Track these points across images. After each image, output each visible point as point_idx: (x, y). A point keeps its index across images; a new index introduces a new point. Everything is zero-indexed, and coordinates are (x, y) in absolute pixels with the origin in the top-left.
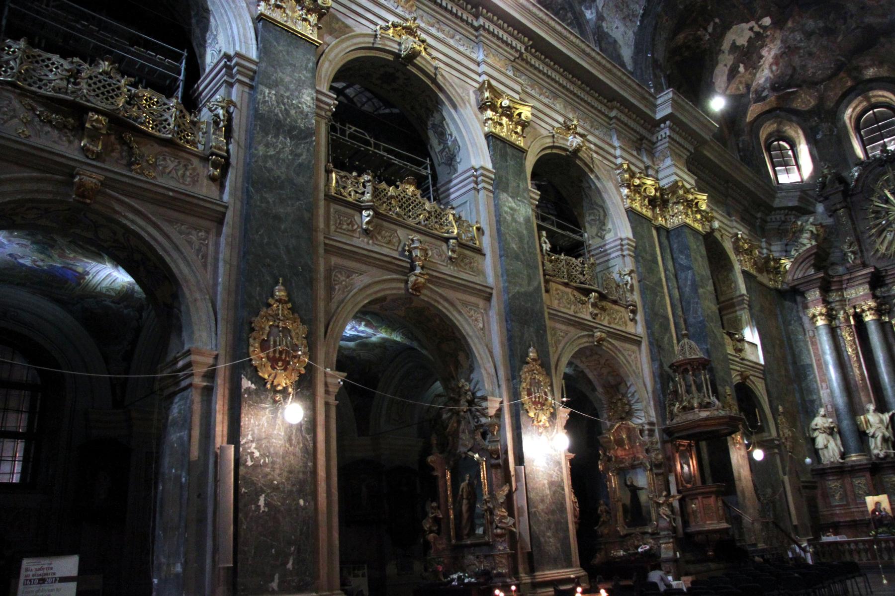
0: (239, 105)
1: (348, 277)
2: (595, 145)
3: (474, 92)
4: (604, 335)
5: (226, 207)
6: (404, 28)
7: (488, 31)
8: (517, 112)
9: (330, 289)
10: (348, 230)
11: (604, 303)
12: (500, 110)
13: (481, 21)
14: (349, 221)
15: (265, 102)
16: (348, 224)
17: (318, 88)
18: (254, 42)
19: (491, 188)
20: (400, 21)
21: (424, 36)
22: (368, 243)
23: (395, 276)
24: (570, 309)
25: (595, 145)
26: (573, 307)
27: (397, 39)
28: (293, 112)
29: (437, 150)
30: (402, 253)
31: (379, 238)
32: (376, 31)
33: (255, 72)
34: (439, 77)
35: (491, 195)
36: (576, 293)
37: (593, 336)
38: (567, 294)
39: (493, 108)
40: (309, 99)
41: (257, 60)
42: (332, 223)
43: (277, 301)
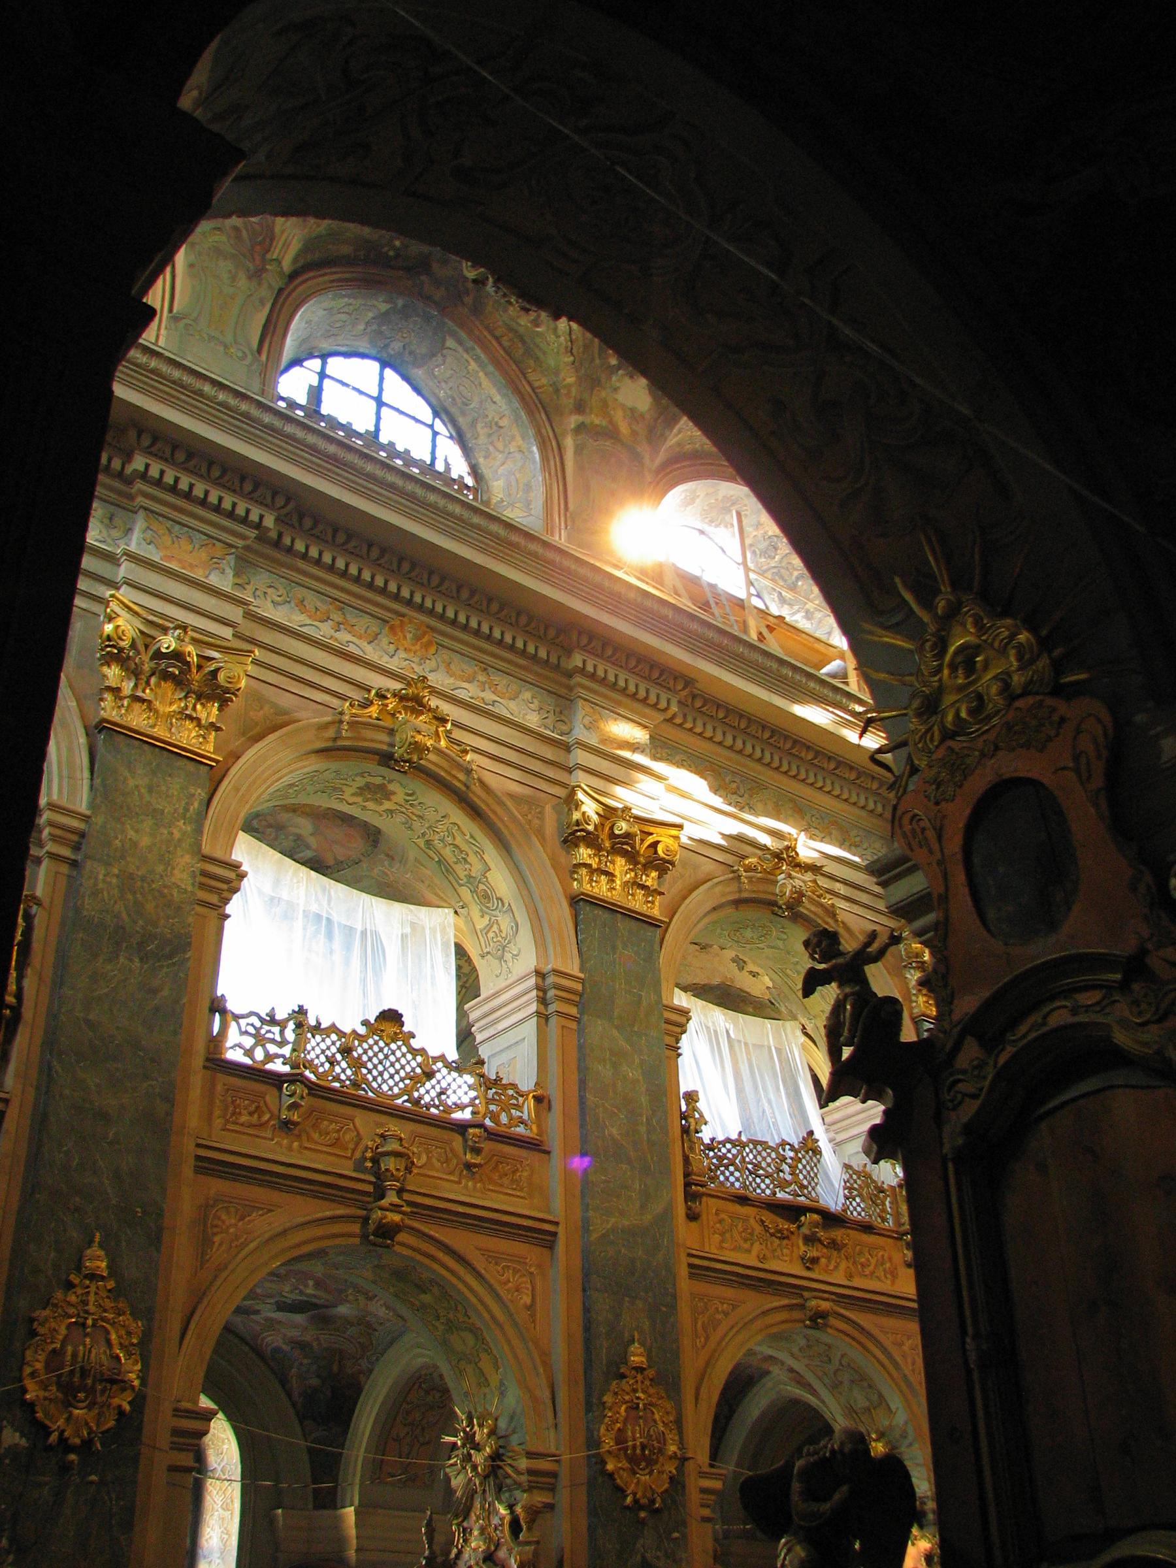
0: (46, 902)
1: (242, 1218)
2: (845, 882)
3: (554, 808)
4: (825, 1305)
5: (6, 1101)
6: (403, 698)
7: (593, 676)
8: (650, 840)
9: (204, 1241)
10: (251, 1126)
11: (838, 1234)
12: (607, 844)
13: (577, 660)
14: (253, 1108)
15: (95, 893)
16: (251, 1114)
17: (206, 849)
18: (87, 774)
19: (574, 1011)
20: (397, 686)
21: (446, 708)
22: (290, 1148)
23: (341, 1211)
24: (749, 1251)
25: (845, 882)
26: (757, 1246)
27: (387, 723)
28: (150, 906)
29: (478, 927)
30: (359, 1166)
31: (316, 1136)
32: (341, 713)
33: (82, 835)
34: (477, 788)
35: (574, 1025)
36: (768, 1217)
37: (802, 1307)
38: (746, 1220)
39: (591, 840)
40: (185, 876)
41: (88, 813)
42: (217, 1112)
43: (86, 1277)
